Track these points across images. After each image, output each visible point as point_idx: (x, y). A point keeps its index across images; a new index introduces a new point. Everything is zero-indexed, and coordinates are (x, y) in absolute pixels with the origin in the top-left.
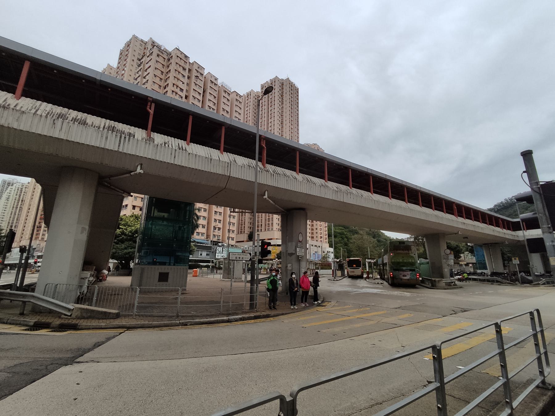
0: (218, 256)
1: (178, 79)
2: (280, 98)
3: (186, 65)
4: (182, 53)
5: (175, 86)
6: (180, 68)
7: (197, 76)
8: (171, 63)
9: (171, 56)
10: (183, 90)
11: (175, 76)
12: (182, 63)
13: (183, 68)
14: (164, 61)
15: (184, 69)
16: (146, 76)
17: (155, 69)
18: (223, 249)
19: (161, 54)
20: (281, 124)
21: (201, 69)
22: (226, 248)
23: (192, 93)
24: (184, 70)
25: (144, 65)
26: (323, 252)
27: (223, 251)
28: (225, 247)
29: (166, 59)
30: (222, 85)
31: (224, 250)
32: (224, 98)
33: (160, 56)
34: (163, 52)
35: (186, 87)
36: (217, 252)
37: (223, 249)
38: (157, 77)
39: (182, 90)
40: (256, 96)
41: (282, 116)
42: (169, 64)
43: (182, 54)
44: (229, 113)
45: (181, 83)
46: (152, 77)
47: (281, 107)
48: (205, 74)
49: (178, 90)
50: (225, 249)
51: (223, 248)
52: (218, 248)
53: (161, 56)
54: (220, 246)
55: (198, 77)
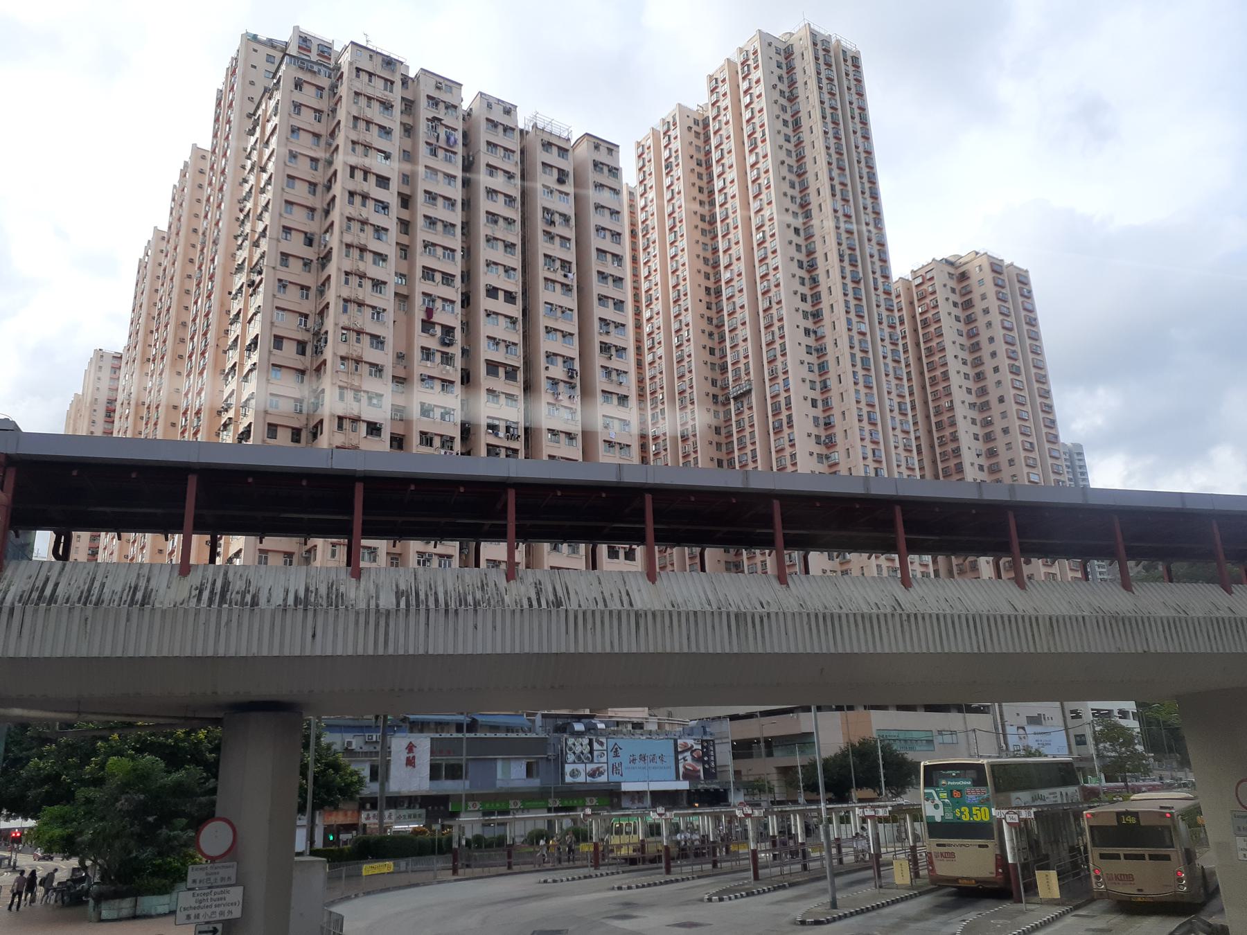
0: (574, 774)
1: (367, 147)
2: (784, 109)
4: (373, 54)
5: (359, 175)
6: (369, 106)
7: (435, 119)
10: (388, 179)
11: (355, 139)
12: (377, 89)
13: (382, 103)
15: (387, 106)
17: (293, 131)
18: (591, 744)
19: (306, 77)
20: (802, 206)
22: (604, 740)
24: (387, 109)
26: (1069, 715)
27: (591, 752)
28: (602, 735)
29: (327, 89)
30: (535, 126)
31: (596, 746)
32: (548, 170)
33: (305, 86)
34: (316, 68)
36: (571, 757)
37: (591, 744)
38: (300, 157)
39: (383, 181)
40: (696, 122)
41: (799, 176)
43: (374, 56)
44: (573, 222)
45: (380, 156)
47: (793, 144)
48: (465, 106)
50: (601, 744)
51: (591, 740)
52: (571, 741)
54: (579, 734)
55: (440, 120)
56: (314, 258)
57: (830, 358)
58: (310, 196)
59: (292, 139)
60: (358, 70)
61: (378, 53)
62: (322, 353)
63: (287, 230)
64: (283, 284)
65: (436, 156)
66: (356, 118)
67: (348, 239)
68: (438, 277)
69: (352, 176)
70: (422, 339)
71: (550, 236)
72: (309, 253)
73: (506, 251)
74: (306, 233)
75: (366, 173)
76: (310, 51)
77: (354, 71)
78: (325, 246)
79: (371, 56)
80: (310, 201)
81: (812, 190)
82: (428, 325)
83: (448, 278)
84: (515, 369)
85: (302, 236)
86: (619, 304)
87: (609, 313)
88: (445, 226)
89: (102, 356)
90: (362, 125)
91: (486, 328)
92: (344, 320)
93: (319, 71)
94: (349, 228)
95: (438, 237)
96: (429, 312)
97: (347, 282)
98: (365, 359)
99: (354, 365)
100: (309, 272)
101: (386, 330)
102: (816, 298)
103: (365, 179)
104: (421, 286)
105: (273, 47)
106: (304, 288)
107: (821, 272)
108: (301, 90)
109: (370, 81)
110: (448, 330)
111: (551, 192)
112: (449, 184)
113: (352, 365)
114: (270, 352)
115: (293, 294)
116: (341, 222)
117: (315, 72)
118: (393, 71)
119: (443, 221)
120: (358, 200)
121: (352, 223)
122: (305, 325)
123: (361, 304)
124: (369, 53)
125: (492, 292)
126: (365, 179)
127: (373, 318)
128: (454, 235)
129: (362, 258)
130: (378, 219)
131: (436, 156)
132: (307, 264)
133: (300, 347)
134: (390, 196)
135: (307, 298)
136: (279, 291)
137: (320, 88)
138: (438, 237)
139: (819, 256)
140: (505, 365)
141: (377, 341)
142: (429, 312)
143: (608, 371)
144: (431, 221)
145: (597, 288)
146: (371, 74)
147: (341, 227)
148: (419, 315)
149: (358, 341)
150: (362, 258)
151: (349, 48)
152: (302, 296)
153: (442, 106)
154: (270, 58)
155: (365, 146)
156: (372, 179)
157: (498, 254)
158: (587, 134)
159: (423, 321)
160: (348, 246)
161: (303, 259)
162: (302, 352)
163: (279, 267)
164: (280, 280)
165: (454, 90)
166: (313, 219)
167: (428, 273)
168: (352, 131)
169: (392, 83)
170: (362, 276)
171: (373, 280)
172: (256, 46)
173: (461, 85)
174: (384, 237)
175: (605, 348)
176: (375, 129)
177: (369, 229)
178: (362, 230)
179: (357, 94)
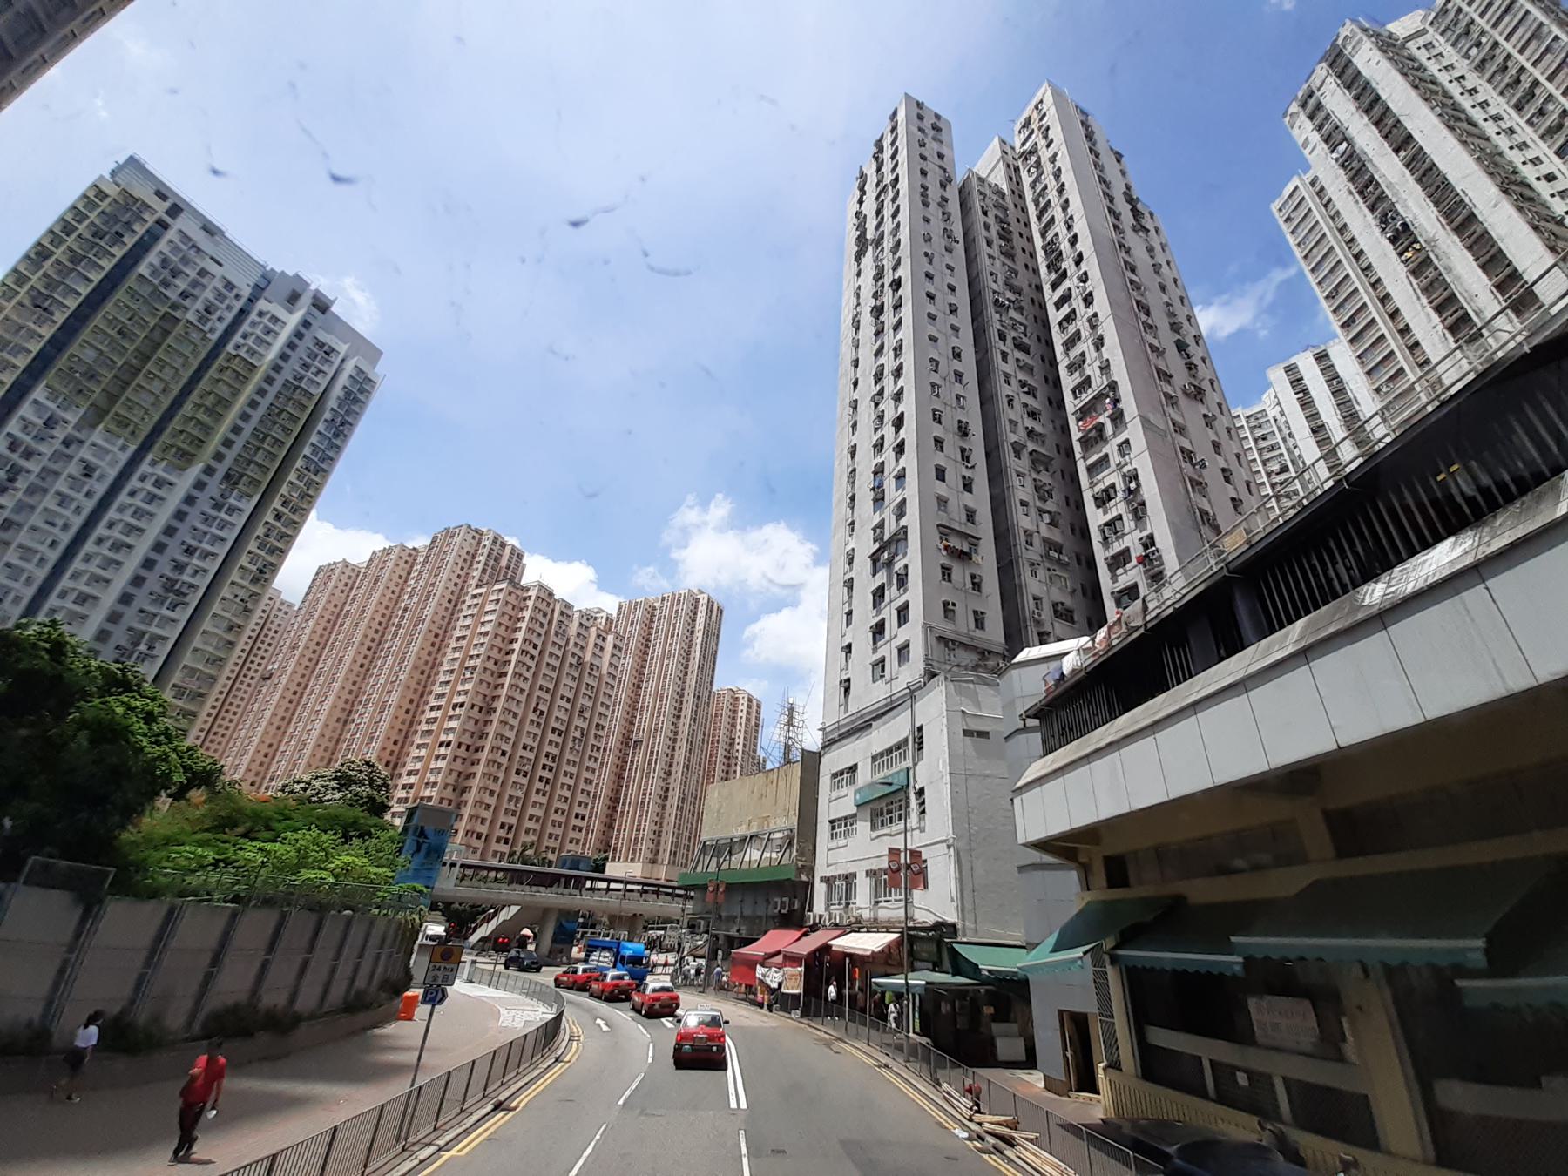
12: (543, 606)
23: (549, 649)
39: (535, 647)
57: (679, 737)
64: (481, 681)
70: (532, 716)
72: (494, 668)
80: (501, 645)
81: (690, 664)
82: (535, 710)
83: (548, 691)
86: (608, 707)
87: (603, 710)
91: (556, 713)
101: (520, 711)
102: (680, 710)
107: (685, 700)
125: (562, 698)
139: (686, 692)
143: (596, 736)
145: (602, 699)
148: (534, 705)
154: (474, 538)
157: (569, 682)
175: (598, 725)
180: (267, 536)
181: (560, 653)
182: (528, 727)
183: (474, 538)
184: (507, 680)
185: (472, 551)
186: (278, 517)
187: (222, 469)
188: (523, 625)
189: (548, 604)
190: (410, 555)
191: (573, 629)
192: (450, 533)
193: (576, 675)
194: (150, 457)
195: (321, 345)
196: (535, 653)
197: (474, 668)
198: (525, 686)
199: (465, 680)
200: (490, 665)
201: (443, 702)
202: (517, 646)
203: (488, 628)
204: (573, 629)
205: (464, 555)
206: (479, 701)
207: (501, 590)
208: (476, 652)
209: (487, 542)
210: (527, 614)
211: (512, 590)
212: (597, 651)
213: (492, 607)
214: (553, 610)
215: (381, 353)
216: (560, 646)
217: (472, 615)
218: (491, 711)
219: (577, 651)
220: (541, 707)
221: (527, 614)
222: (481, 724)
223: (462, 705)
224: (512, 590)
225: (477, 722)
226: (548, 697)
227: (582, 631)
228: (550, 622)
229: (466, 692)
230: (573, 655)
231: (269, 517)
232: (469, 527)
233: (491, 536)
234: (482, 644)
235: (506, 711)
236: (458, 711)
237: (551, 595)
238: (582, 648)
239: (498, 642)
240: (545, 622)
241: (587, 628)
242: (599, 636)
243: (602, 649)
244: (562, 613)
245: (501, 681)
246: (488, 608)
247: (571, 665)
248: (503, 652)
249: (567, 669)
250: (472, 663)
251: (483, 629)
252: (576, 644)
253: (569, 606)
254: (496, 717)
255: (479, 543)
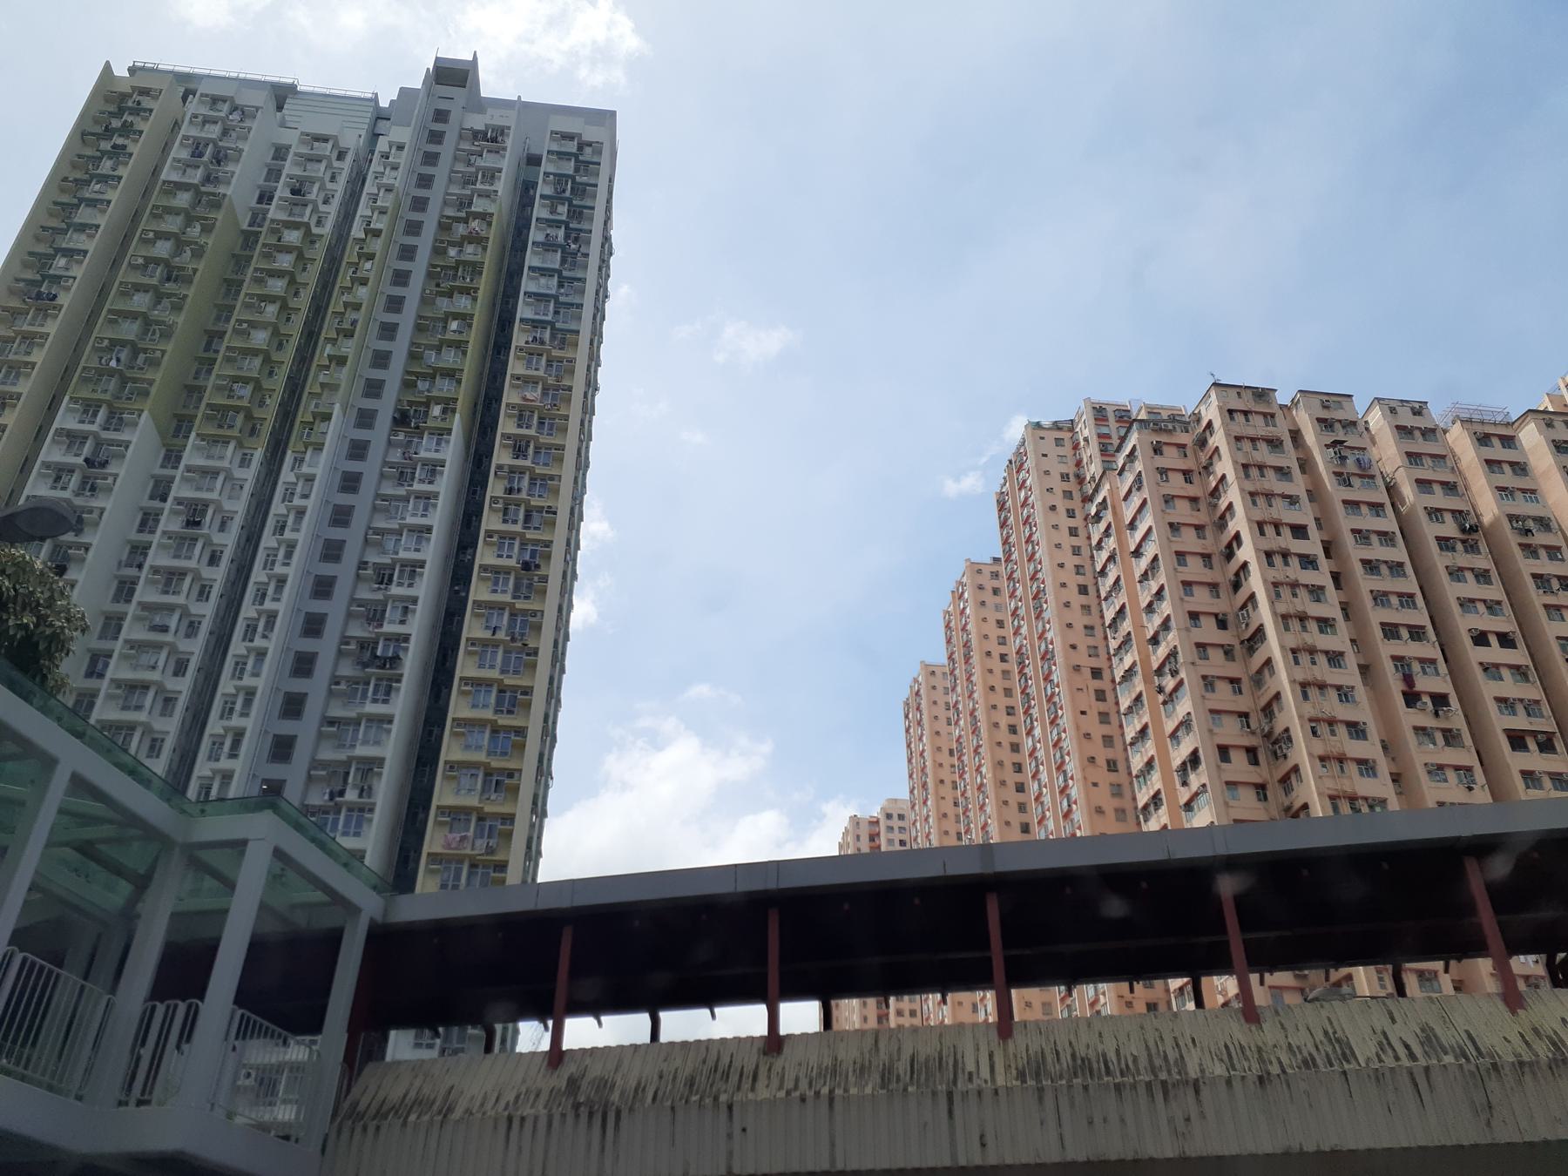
3: (1275, 426)
4: (1239, 389)
7: (1336, 443)
8: (1217, 447)
9: (1204, 423)
11: (1252, 489)
12: (1258, 427)
14: (1185, 456)
16: (1139, 546)
17: (1166, 502)
19: (1164, 438)
21: (1340, 406)
23: (1346, 523)
24: (1276, 446)
25: (1114, 508)
33: (1165, 449)
35: (1312, 508)
39: (1299, 531)
42: (1211, 458)
46: (1168, 539)
49: (1287, 541)
53: (1166, 444)
55: (1341, 442)
56: (1236, 643)
58: (1207, 571)
59: (1168, 511)
60: (1231, 412)
61: (1246, 387)
62: (1285, 756)
63: (1194, 616)
64: (1208, 682)
65: (1350, 485)
66: (1245, 467)
67: (1282, 608)
68: (1404, 633)
69: (1262, 533)
70: (1410, 718)
71: (1530, 550)
73: (1478, 582)
74: (1216, 615)
75: (1277, 526)
76: (1107, 420)
77: (1227, 414)
78: (1247, 625)
79: (1239, 394)
80: (1207, 576)
82: (1411, 698)
83: (1416, 633)
84: (1550, 736)
85: (1213, 620)
88: (1390, 568)
89: (858, 823)
90: (1254, 472)
91: (1489, 690)
92: (1309, 710)
93: (1174, 427)
94: (1278, 595)
95: (1386, 583)
96: (1408, 679)
97: (1297, 662)
98: (1350, 755)
99: (1338, 765)
100: (1234, 660)
101: (1362, 711)
103: (1278, 534)
104: (1387, 649)
105: (1060, 429)
106: (1234, 681)
108: (1161, 454)
109: (1247, 420)
110: (1440, 700)
111: (1512, 493)
112: (1378, 516)
113: (1335, 766)
114: (1218, 767)
115: (1223, 693)
116: (1267, 590)
117: (1170, 431)
118: (1269, 403)
119: (1386, 562)
120: (1278, 560)
121: (1281, 589)
122: (1249, 727)
123: (1322, 687)
124: (1234, 391)
125: (1481, 639)
126: (1278, 534)
127: (1341, 701)
128: (1404, 575)
129: (1304, 628)
130: (1308, 577)
131: (1350, 485)
132: (1228, 652)
133: (1251, 754)
134: (1313, 546)
135: (1240, 692)
136: (1207, 690)
137: (1182, 446)
138: (1386, 583)
140: (1534, 733)
141: (1357, 731)
142: (1408, 679)
144: (1370, 566)
146: (1246, 413)
147: (1269, 596)
148: (1396, 686)
149: (1333, 733)
150: (1304, 628)
151: (1213, 395)
152: (1235, 692)
153: (1337, 426)
154: (1059, 442)
155: (1267, 495)
156: (1286, 532)
157: (1471, 588)
158: (1529, 410)
159: (1404, 693)
160: (1285, 617)
161: (1222, 646)
162: (1255, 761)
163: (1199, 662)
164: (1204, 677)
165: (1345, 404)
166: (1218, 597)
167: (1390, 631)
168: (1246, 482)
169: (1273, 416)
170: (1312, 651)
171: (1326, 653)
172: (1042, 433)
173: (1350, 396)
174: (1322, 597)
176: (1270, 474)
177: (1302, 593)
178: (1295, 595)
179: (1238, 439)
180: (510, 491)
181: (1389, 523)
182: (1421, 755)
183: (1059, 442)
184: (1273, 645)
185: (1070, 469)
186: (519, 450)
187: (386, 409)
188: (1233, 495)
189: (1269, 417)
190: (995, 575)
191: (1388, 454)
192: (1017, 464)
193: (1483, 562)
194: (289, 457)
195: (476, 135)
196: (1313, 546)
197: (1173, 654)
198: (1338, 640)
199: (1171, 698)
200: (1208, 631)
201: (1156, 781)
202: (1246, 553)
203: (1150, 550)
204: (1388, 454)
205: (1059, 486)
206: (1231, 732)
207: (1131, 456)
208: (1157, 620)
209: (1086, 431)
210: (1225, 466)
211: (1155, 438)
212: (1507, 478)
213: (1136, 501)
214: (1296, 435)
215: (613, 114)
216: (1376, 508)
217: (1111, 558)
218: (1278, 743)
219: (1438, 499)
220: (1424, 684)
221: (1225, 466)
222: (1274, 792)
223: (1194, 760)
224: (1155, 438)
225: (1261, 789)
226: (1430, 650)
227: (1420, 445)
228: (1306, 465)
229: (1185, 724)
230: (1435, 513)
231: (502, 456)
232: (1038, 426)
233: (1088, 417)
234: (1159, 594)
235: (1315, 726)
236: (1195, 780)
237: (1262, 394)
238: (1450, 488)
239: (1194, 570)
240: (1289, 459)
241: (1429, 433)
242: (1483, 440)
243: (1520, 468)
244: (1325, 424)
245: (1258, 659)
246: (1128, 513)
247: (1445, 543)
248: (1224, 590)
249: (1440, 561)
250: (1162, 651)
251: (1144, 563)
252: (1423, 485)
253: (1330, 400)
254: (1302, 752)
255: (1076, 447)
